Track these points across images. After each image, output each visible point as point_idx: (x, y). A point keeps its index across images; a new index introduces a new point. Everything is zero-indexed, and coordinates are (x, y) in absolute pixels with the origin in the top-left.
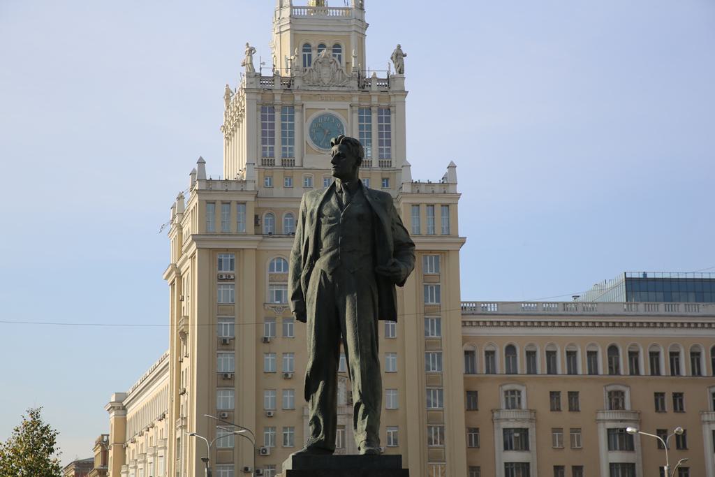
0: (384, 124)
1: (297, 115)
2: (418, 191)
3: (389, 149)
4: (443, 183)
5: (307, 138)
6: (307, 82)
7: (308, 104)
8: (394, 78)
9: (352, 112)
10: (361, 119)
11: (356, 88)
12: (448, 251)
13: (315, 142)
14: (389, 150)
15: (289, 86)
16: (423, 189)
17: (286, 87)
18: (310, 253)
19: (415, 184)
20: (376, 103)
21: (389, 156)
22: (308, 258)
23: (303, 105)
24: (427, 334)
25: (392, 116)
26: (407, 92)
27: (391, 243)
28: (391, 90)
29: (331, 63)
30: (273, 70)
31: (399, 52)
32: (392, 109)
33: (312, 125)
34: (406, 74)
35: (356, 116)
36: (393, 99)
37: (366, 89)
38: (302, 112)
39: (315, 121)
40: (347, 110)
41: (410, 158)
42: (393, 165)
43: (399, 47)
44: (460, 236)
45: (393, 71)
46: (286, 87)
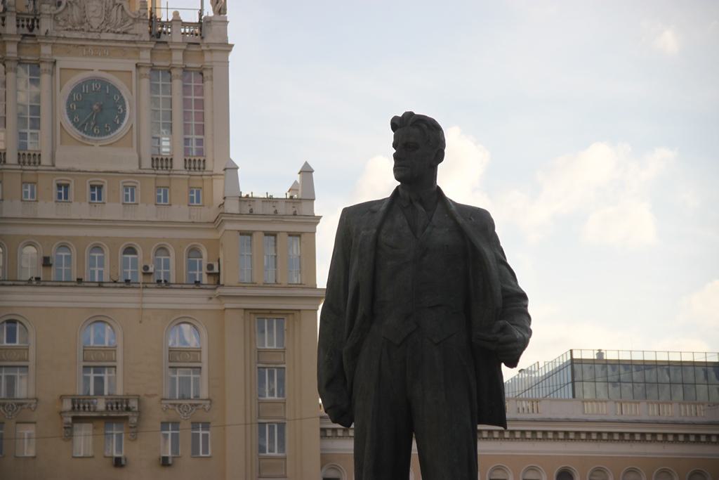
0: (193, 97)
1: (45, 78)
2: (251, 211)
3: (202, 140)
4: (291, 197)
6: (62, 23)
7: (64, 62)
8: (209, 21)
9: (140, 77)
11: (147, 37)
12: (299, 310)
13: (75, 124)
14: (200, 142)
15: (31, 29)
16: (258, 209)
17: (25, 31)
18: (362, 309)
19: (249, 200)
20: (181, 63)
21: (200, 152)
22: (359, 317)
23: (55, 63)
24: (262, 449)
25: (208, 83)
26: (232, 46)
27: (499, 294)
28: (205, 41)
30: (201, 15)
32: (206, 73)
33: (71, 96)
34: (230, 15)
35: (145, 83)
36: (207, 57)
37: (164, 38)
38: (52, 73)
39: (78, 88)
40: (131, 72)
41: (236, 154)
42: (209, 166)
44: (318, 287)
45: (209, 11)
46: (25, 31)
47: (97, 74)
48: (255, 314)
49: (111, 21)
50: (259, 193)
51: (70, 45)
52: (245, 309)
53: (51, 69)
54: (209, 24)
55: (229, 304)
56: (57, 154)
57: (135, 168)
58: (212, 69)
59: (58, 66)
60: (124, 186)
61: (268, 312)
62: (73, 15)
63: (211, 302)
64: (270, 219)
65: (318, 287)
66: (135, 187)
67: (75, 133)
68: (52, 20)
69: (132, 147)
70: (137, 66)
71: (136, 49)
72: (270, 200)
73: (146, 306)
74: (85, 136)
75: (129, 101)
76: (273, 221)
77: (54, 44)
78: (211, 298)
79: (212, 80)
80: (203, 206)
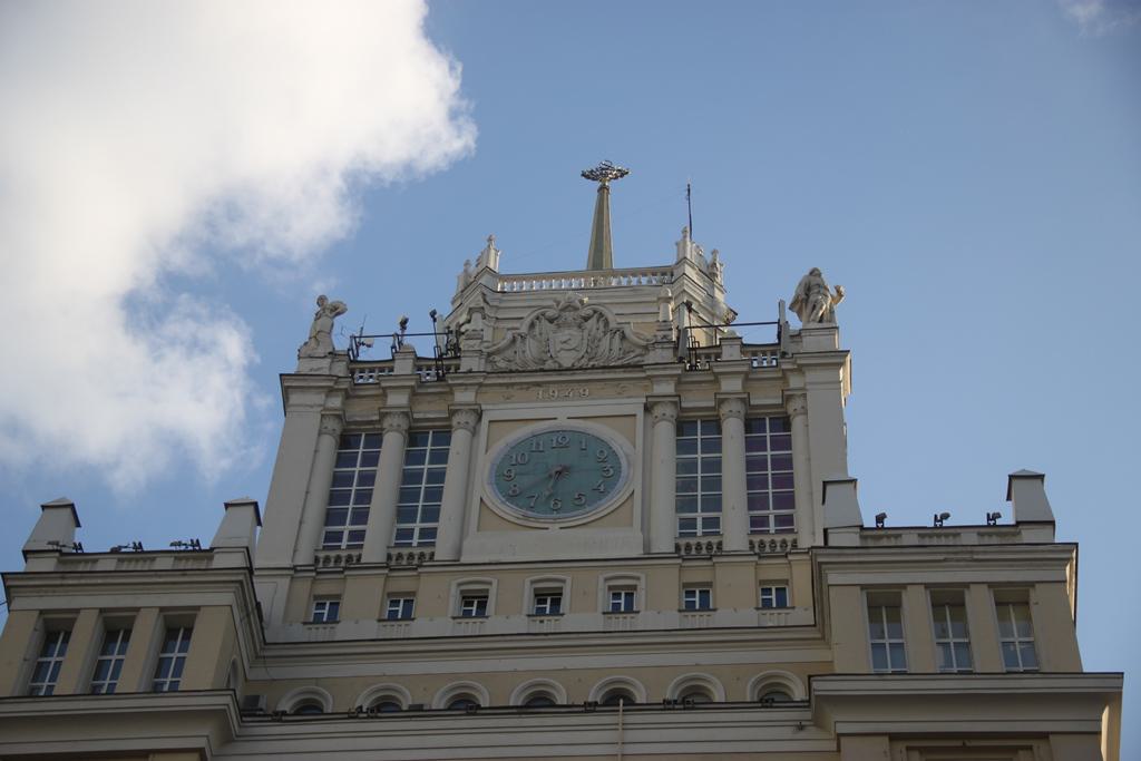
1: (459, 438)
5: (484, 489)
9: (649, 428)
10: (683, 447)
12: (1044, 736)
13: (512, 497)
23: (479, 415)
29: (586, 319)
31: (815, 281)
33: (508, 456)
35: (665, 433)
38: (474, 432)
43: (815, 273)
47: (563, 423)
48: (922, 750)
49: (601, 350)
50: (909, 512)
51: (513, 384)
52: (894, 737)
53: (472, 424)
54: (795, 339)
55: (845, 721)
56: (465, 543)
57: (638, 552)
58: (805, 396)
59: (485, 420)
60: (610, 588)
61: (959, 743)
62: (524, 352)
63: (802, 735)
64: (942, 557)
65: (1085, 671)
66: (635, 587)
67: (508, 511)
68: (483, 361)
69: (631, 525)
70: (648, 409)
71: (647, 383)
72: (940, 533)
73: (630, 749)
74: (530, 513)
75: (627, 456)
76: (945, 560)
77: (481, 385)
78: (801, 728)
79: (806, 413)
80: (793, 608)
